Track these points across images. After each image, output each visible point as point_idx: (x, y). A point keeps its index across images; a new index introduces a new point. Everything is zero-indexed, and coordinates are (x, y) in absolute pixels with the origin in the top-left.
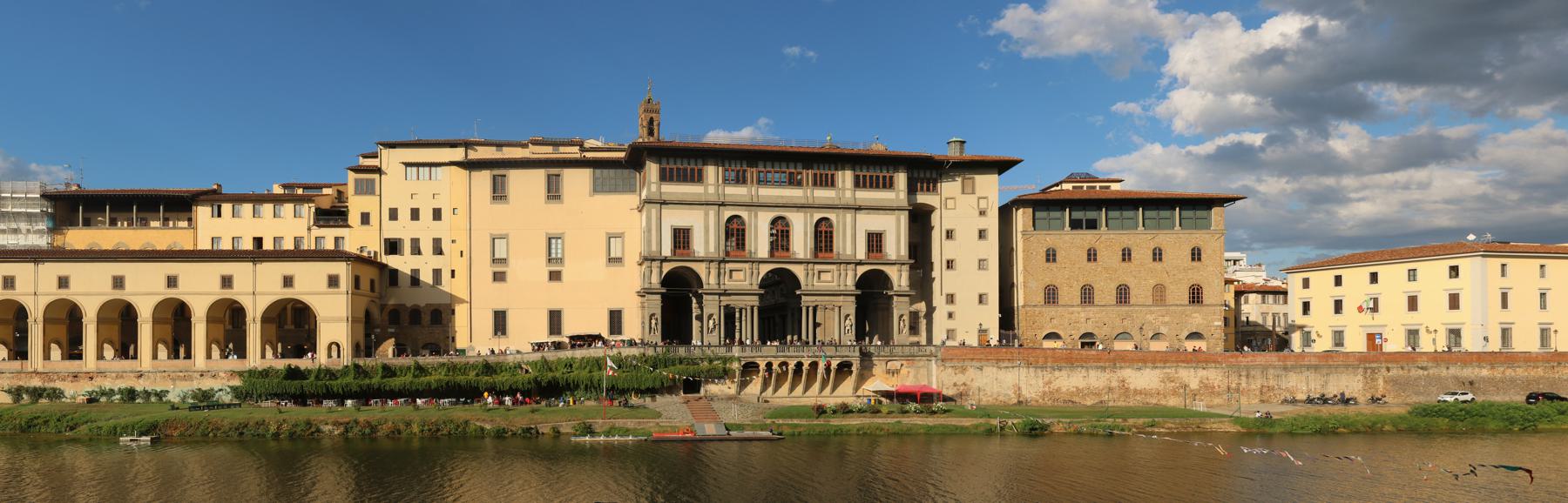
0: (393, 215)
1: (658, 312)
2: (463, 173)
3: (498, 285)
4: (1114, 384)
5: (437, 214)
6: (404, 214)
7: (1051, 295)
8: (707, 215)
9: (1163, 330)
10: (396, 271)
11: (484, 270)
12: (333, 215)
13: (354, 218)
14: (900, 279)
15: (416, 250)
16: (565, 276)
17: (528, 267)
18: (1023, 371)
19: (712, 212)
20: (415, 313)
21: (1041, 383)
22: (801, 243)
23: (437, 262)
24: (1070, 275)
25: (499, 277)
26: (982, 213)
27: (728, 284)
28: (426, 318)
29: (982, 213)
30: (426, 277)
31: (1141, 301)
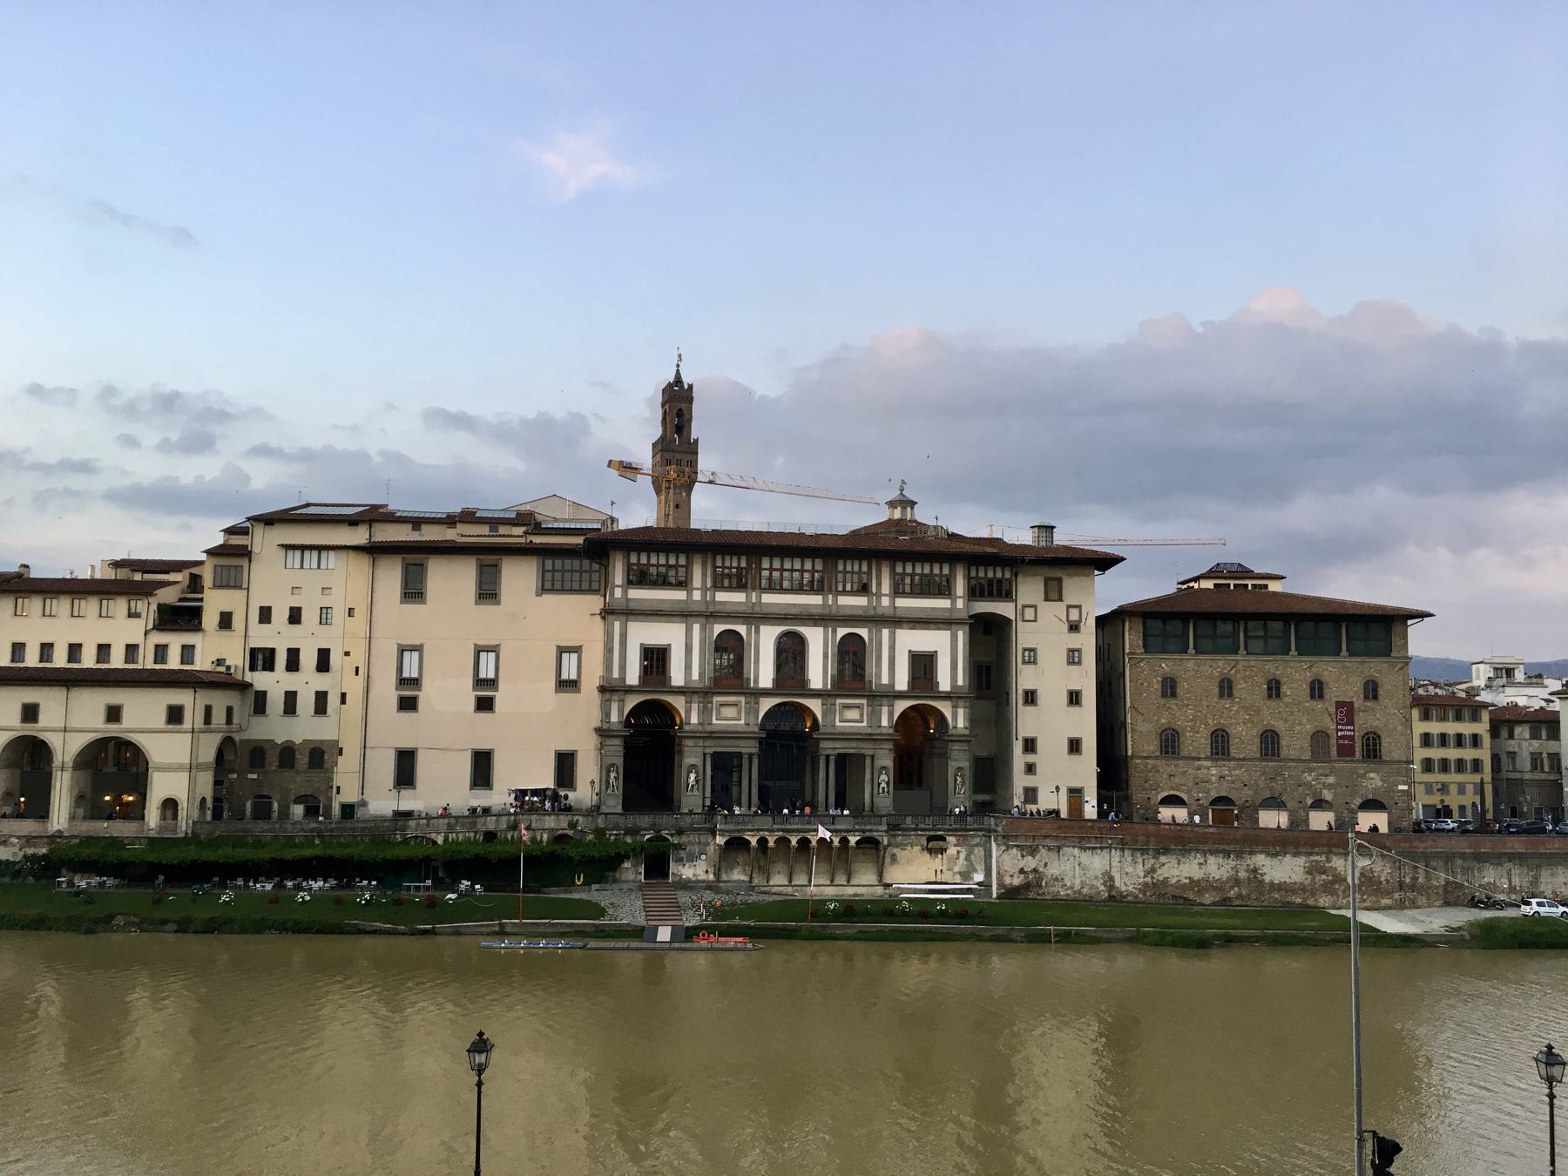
0: (265, 615)
1: (620, 761)
2: (361, 564)
4: (1243, 875)
6: (280, 615)
7: (1170, 743)
9: (1328, 795)
11: (386, 692)
12: (182, 617)
13: (210, 619)
14: (958, 719)
16: (499, 704)
17: (447, 691)
18: (1116, 854)
21: (1140, 870)
22: (817, 673)
23: (321, 682)
24: (1194, 719)
25: (408, 704)
26: (1074, 627)
28: (302, 760)
29: (1074, 627)
31: (1293, 754)
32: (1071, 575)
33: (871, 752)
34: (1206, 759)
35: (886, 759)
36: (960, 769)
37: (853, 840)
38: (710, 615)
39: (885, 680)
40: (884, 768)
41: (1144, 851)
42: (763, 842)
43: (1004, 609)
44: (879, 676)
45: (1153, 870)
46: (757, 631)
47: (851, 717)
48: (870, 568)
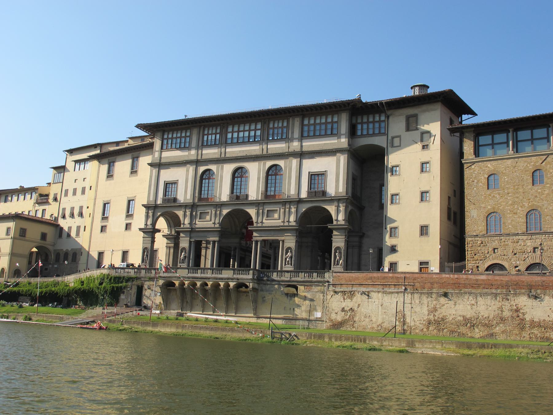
2: (95, 163)
3: (102, 234)
4: (507, 314)
5: (83, 192)
6: (70, 193)
8: (188, 171)
10: (62, 228)
14: (339, 215)
15: (72, 215)
18: (408, 297)
19: (191, 169)
20: (66, 255)
21: (425, 310)
25: (103, 229)
27: (199, 224)
30: (73, 234)
32: (424, 111)
33: (283, 238)
34: (523, 234)
35: (290, 242)
36: (338, 248)
37: (232, 284)
38: (197, 163)
39: (293, 191)
40: (289, 248)
41: (430, 294)
44: (289, 190)
45: (435, 310)
46: (222, 169)
48: (288, 123)
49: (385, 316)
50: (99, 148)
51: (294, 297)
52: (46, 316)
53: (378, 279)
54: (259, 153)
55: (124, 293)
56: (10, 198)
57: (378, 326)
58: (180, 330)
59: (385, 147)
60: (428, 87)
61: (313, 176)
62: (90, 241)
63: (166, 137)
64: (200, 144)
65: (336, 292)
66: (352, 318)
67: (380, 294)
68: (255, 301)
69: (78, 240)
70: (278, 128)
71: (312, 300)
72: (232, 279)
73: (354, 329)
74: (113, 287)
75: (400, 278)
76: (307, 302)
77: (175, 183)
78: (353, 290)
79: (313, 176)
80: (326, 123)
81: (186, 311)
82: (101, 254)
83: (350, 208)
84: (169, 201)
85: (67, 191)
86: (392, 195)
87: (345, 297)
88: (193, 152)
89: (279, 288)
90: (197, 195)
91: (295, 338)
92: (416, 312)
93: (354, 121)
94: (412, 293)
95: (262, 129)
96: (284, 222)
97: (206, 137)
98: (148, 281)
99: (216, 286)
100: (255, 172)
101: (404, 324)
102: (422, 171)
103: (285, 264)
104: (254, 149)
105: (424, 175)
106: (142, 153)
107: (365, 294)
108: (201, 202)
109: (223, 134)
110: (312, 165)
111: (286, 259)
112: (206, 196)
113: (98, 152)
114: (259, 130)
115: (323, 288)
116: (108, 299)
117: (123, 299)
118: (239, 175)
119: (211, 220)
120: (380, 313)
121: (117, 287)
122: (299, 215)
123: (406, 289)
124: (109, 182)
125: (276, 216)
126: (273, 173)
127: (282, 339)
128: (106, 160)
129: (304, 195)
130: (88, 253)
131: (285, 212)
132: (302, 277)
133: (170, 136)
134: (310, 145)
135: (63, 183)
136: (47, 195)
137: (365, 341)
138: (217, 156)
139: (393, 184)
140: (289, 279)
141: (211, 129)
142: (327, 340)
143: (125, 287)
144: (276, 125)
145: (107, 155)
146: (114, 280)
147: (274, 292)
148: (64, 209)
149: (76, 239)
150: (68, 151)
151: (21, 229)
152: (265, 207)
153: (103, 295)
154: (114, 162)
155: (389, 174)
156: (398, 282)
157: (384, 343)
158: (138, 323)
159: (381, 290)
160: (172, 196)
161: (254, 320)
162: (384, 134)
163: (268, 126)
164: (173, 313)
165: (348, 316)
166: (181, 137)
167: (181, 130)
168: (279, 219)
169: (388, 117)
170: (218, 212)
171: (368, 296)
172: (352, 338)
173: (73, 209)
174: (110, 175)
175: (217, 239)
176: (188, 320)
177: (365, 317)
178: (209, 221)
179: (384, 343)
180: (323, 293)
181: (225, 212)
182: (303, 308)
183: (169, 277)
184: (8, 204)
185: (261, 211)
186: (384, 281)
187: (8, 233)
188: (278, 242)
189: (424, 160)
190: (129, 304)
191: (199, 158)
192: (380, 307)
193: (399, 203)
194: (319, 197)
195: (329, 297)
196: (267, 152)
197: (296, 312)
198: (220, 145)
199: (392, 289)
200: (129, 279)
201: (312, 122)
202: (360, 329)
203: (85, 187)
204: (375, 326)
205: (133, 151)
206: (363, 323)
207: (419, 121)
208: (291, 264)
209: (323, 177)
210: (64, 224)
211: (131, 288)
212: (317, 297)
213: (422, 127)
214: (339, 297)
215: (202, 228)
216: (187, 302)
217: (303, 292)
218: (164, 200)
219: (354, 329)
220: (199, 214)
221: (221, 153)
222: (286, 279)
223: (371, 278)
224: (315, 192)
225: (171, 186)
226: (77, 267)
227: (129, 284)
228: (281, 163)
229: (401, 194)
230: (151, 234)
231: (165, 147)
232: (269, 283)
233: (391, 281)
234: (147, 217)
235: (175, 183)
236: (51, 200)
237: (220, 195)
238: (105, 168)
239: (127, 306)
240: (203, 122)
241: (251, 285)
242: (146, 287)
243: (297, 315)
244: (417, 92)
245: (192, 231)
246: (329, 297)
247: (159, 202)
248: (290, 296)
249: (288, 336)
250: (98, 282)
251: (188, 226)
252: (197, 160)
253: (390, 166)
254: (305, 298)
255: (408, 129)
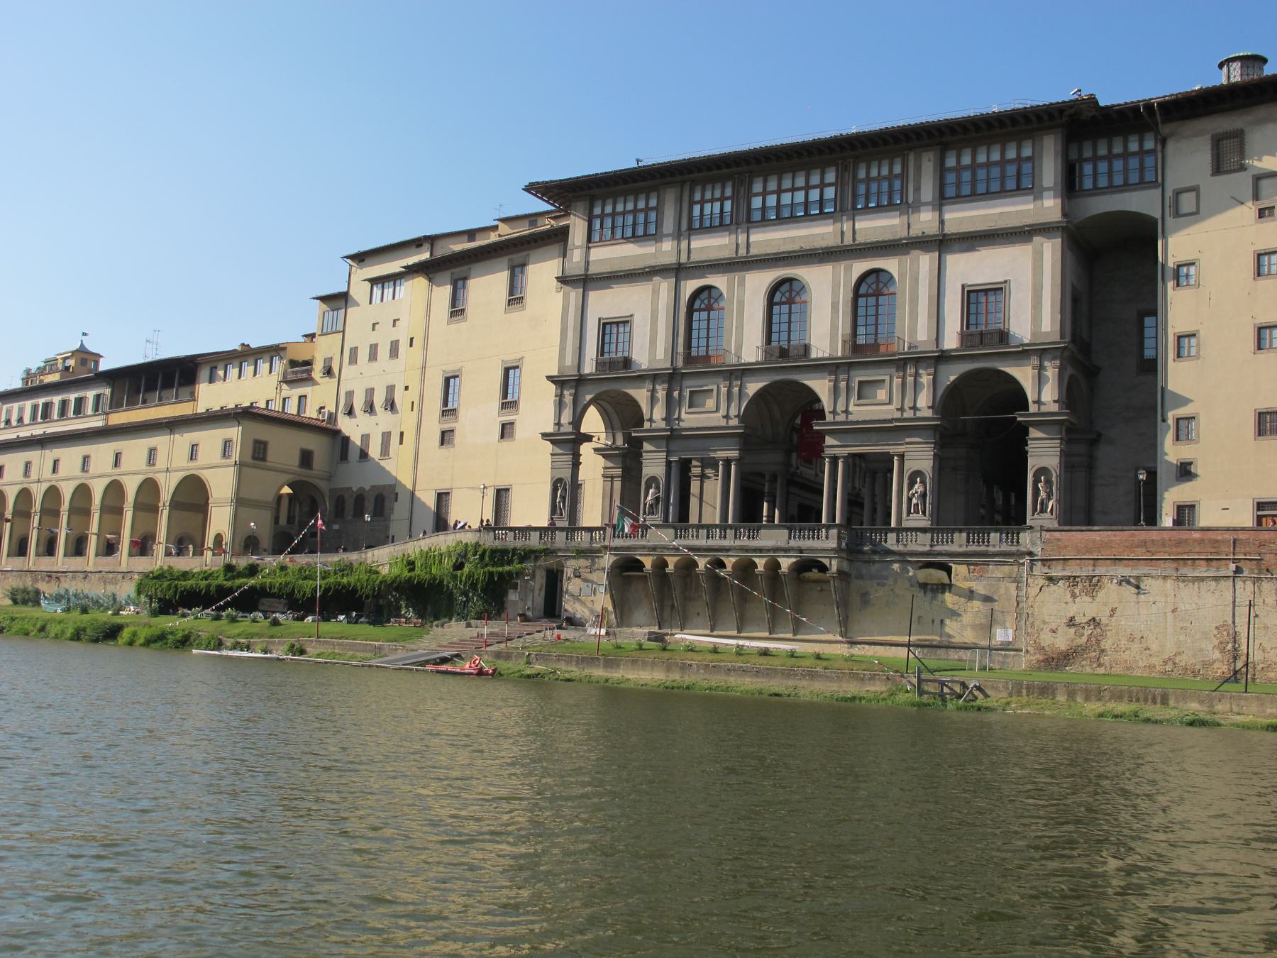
2: (420, 283)
6: (363, 354)
8: (656, 292)
14: (1043, 389)
15: (370, 408)
18: (1245, 591)
19: (664, 286)
20: (360, 499)
22: (824, 332)
25: (446, 437)
27: (689, 419)
30: (374, 451)
33: (900, 449)
35: (919, 457)
37: (786, 563)
38: (678, 271)
39: (922, 335)
40: (918, 473)
42: (661, 565)
43: (1141, 202)
44: (913, 331)
46: (742, 283)
47: (883, 403)
49: (1182, 638)
50: (427, 246)
51: (943, 592)
52: (339, 644)
53: (1164, 545)
54: (833, 241)
55: (515, 587)
56: (221, 373)
57: (1165, 662)
58: (676, 676)
59: (1158, 215)
60: (1264, 61)
61: (974, 296)
62: (416, 468)
63: (597, 211)
64: (684, 226)
65: (1051, 579)
66: (1095, 644)
67: (1169, 582)
68: (844, 604)
69: (387, 465)
70: (879, 179)
71: (988, 599)
72: (786, 550)
73: (1101, 670)
74: (491, 574)
75: (1224, 542)
76: (977, 604)
77: (626, 322)
78: (1097, 572)
79: (974, 296)
80: (1003, 162)
81: (671, 627)
82: (442, 497)
83: (1070, 371)
84: (612, 365)
85: (354, 351)
86: (1179, 337)
87: (1077, 591)
88: (668, 246)
89: (905, 570)
90: (681, 349)
91: (976, 693)
92: (1266, 627)
93: (1073, 155)
94: (1257, 580)
95: (839, 184)
96: (902, 409)
97: (697, 209)
98: (574, 558)
99: (745, 569)
100: (826, 291)
101: (1235, 658)
102: (1259, 275)
103: (909, 513)
104: (822, 233)
105: (1262, 283)
106: (534, 254)
107: (1129, 583)
108: (691, 367)
109: (742, 197)
110: (968, 269)
111: (910, 500)
112: (702, 353)
113: (425, 256)
114: (830, 185)
115: (1015, 568)
116: (476, 603)
117: (515, 602)
118: (784, 296)
119: (717, 410)
120: (1170, 630)
121: (501, 574)
122: (940, 393)
123: (1238, 570)
124: (454, 326)
125: (882, 394)
126: (872, 289)
127: (942, 695)
128: (447, 275)
129: (951, 341)
130: (413, 494)
131: (904, 384)
132: (959, 542)
133: (609, 209)
134: (961, 217)
135: (343, 332)
136: (308, 363)
137: (1165, 700)
138: (728, 253)
139: (1179, 309)
140: (928, 548)
141: (709, 187)
142: (1061, 698)
143: (519, 574)
144: (874, 173)
145: (447, 263)
146: (491, 557)
147: (890, 581)
148: (350, 394)
149: (383, 463)
150: (352, 257)
151: (257, 442)
152: (852, 373)
153: (465, 594)
154: (465, 279)
155: (1170, 284)
156: (1218, 553)
157: (1219, 707)
158: (569, 660)
159: (1170, 572)
160: (620, 355)
161: (842, 650)
162: (1153, 184)
163: (855, 176)
164: (638, 633)
165: (1084, 639)
166: (635, 212)
167: (636, 194)
168: (890, 403)
169: (1164, 142)
170: (736, 390)
171: (1138, 587)
172: (1130, 693)
173: (370, 392)
174: (457, 310)
175: (734, 454)
176: (692, 650)
177: (1131, 639)
178: (714, 412)
179: (1219, 707)
180: (1017, 581)
181: (753, 387)
182: (967, 618)
183: (628, 548)
184: (218, 385)
185: (843, 384)
186: (1180, 550)
187: (226, 453)
188: (888, 458)
189: (1262, 246)
190: (529, 614)
191: (684, 259)
192: (1170, 616)
193: (1198, 356)
194: (991, 346)
195: (1033, 591)
196: (854, 239)
197: (947, 630)
198: (733, 227)
199: (1202, 571)
200: (528, 554)
201: (966, 160)
202: (1117, 670)
203: (397, 341)
204: (1156, 661)
205: (513, 250)
206: (1126, 656)
207: (1247, 148)
208: (924, 513)
209: (1000, 297)
210: (351, 428)
211: (533, 577)
212: (1002, 591)
213: (1256, 164)
214: (1061, 589)
215: (698, 429)
216: (673, 606)
217: (965, 579)
218: (600, 364)
219: (1101, 670)
220: (687, 393)
221: (737, 245)
222: (921, 549)
223: (1143, 544)
224: (981, 334)
225: (615, 330)
226: (387, 528)
227: (529, 565)
228: (890, 264)
229: (1202, 334)
230: (570, 446)
231: (596, 237)
232: (877, 558)
233: (1198, 549)
234: (560, 405)
235: (625, 322)
236: (317, 373)
237: (739, 347)
238: (443, 293)
239: (525, 618)
240: (690, 172)
241: (834, 565)
242: (568, 572)
243: (949, 636)
244: (1236, 74)
245: (672, 437)
246: (1033, 591)
247: (589, 368)
248: (932, 590)
249: (958, 689)
250: (451, 563)
251: (663, 425)
252: (680, 264)
253: (1171, 264)
254: (971, 595)
255: (1218, 169)
